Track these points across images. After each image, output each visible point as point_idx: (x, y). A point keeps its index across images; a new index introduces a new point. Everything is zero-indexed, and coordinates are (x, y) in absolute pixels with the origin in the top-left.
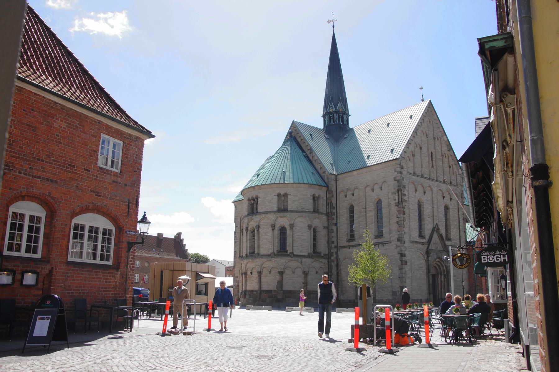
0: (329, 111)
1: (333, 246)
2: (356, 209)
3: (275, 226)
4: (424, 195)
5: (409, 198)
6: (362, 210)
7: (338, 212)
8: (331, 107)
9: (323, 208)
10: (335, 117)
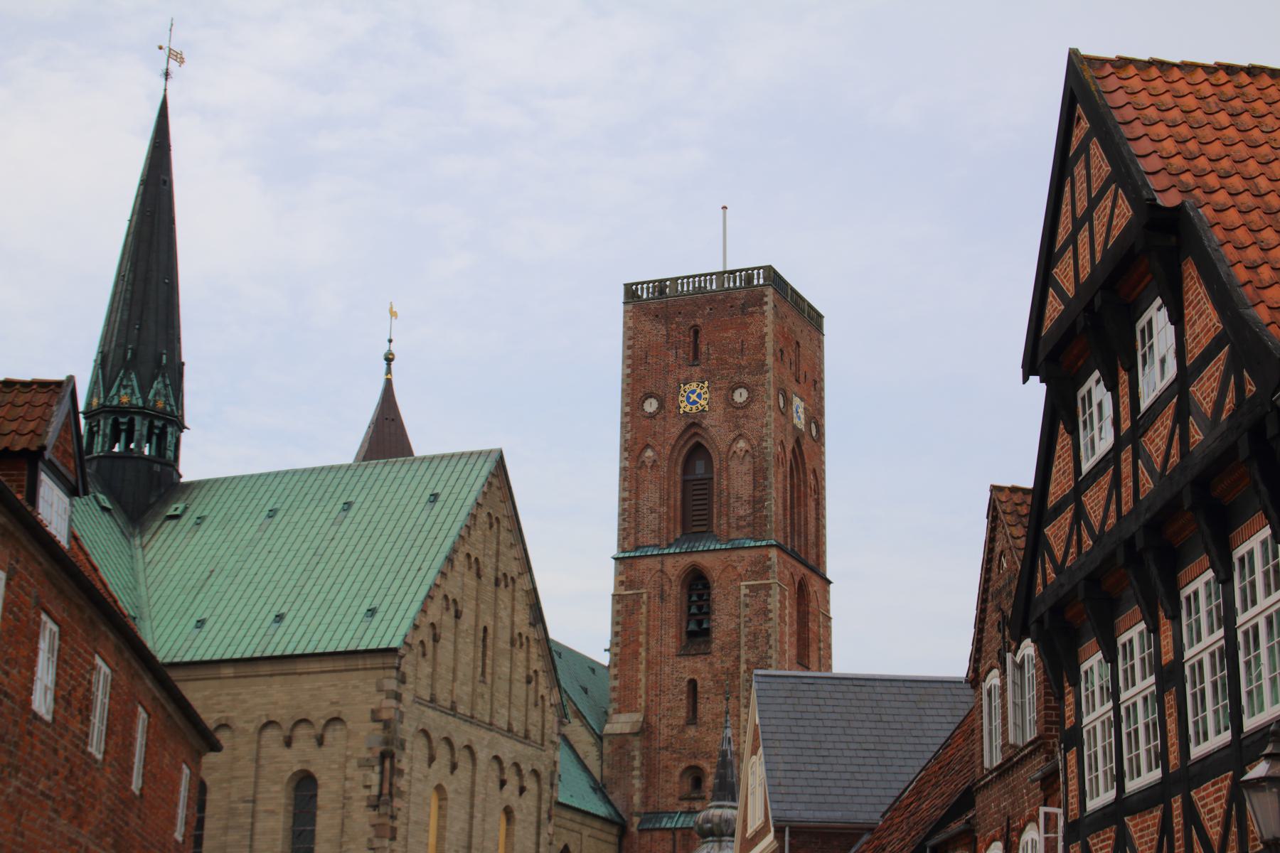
10: (137, 427)
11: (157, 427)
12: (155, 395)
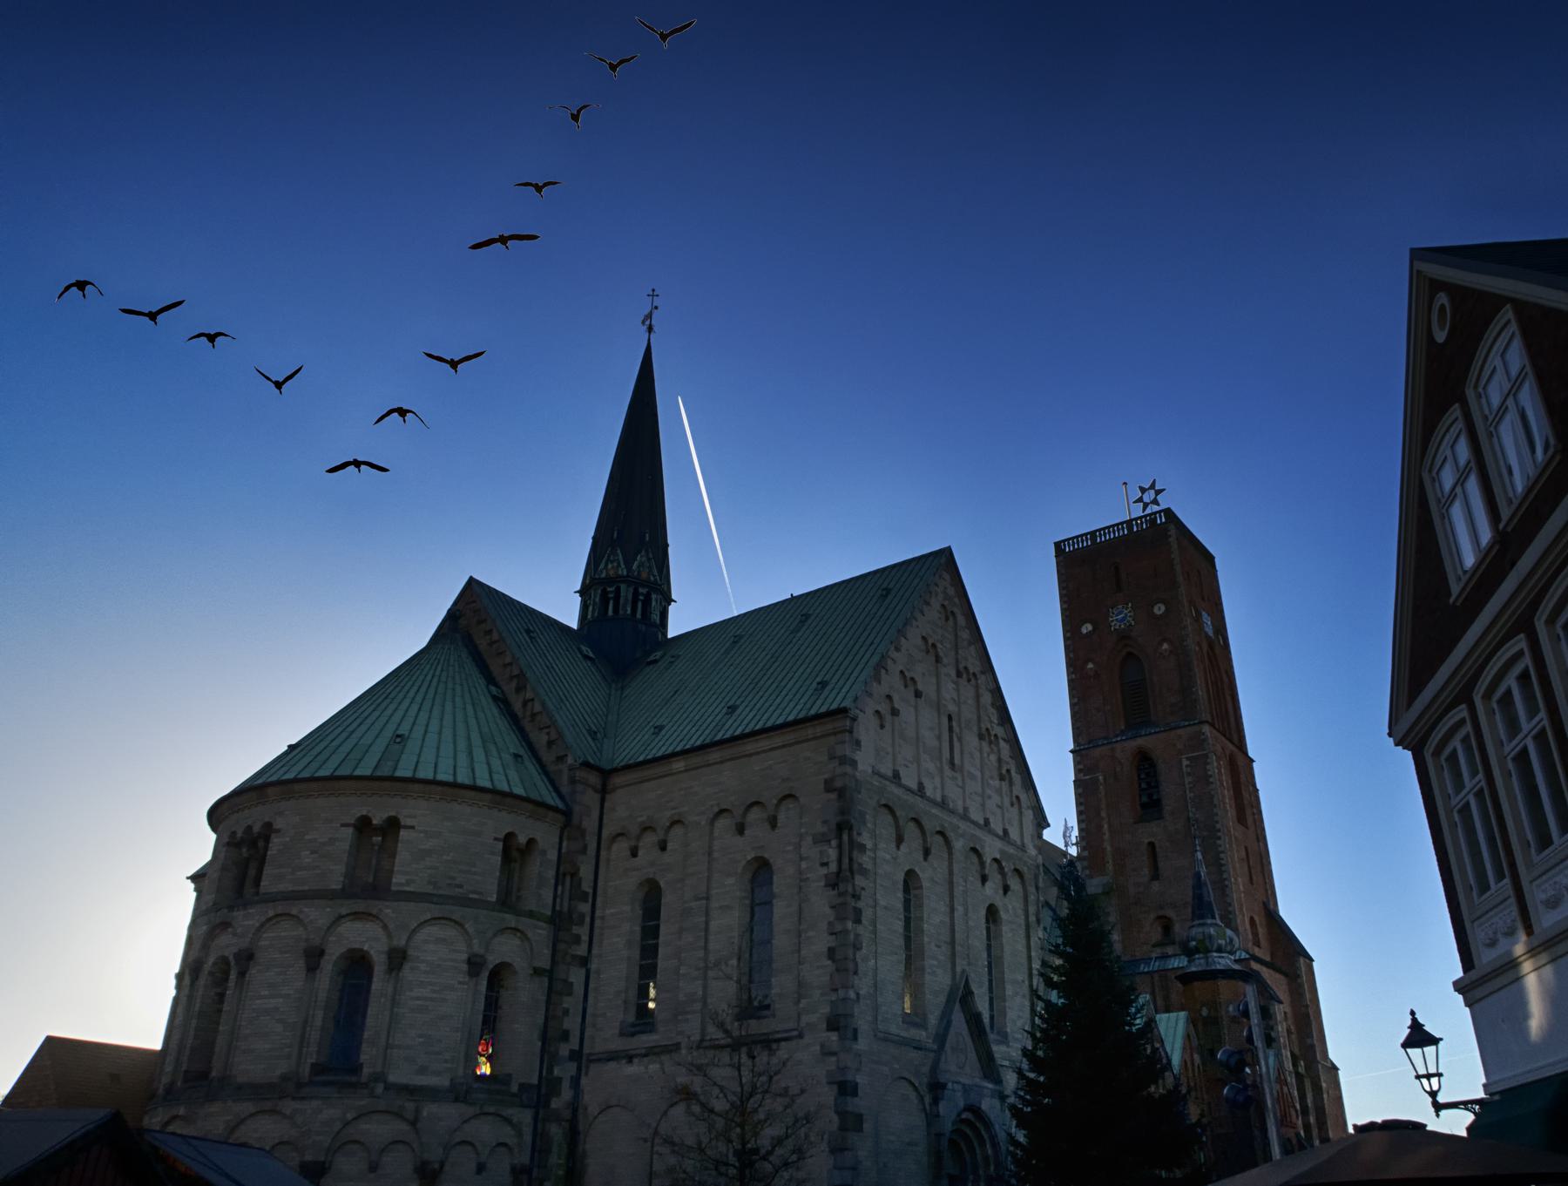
0: (603, 575)
1: (564, 1050)
2: (668, 900)
3: (322, 953)
4: (925, 859)
5: (875, 859)
6: (693, 904)
7: (598, 913)
8: (612, 562)
9: (539, 890)
11: (642, 594)
12: (639, 567)
